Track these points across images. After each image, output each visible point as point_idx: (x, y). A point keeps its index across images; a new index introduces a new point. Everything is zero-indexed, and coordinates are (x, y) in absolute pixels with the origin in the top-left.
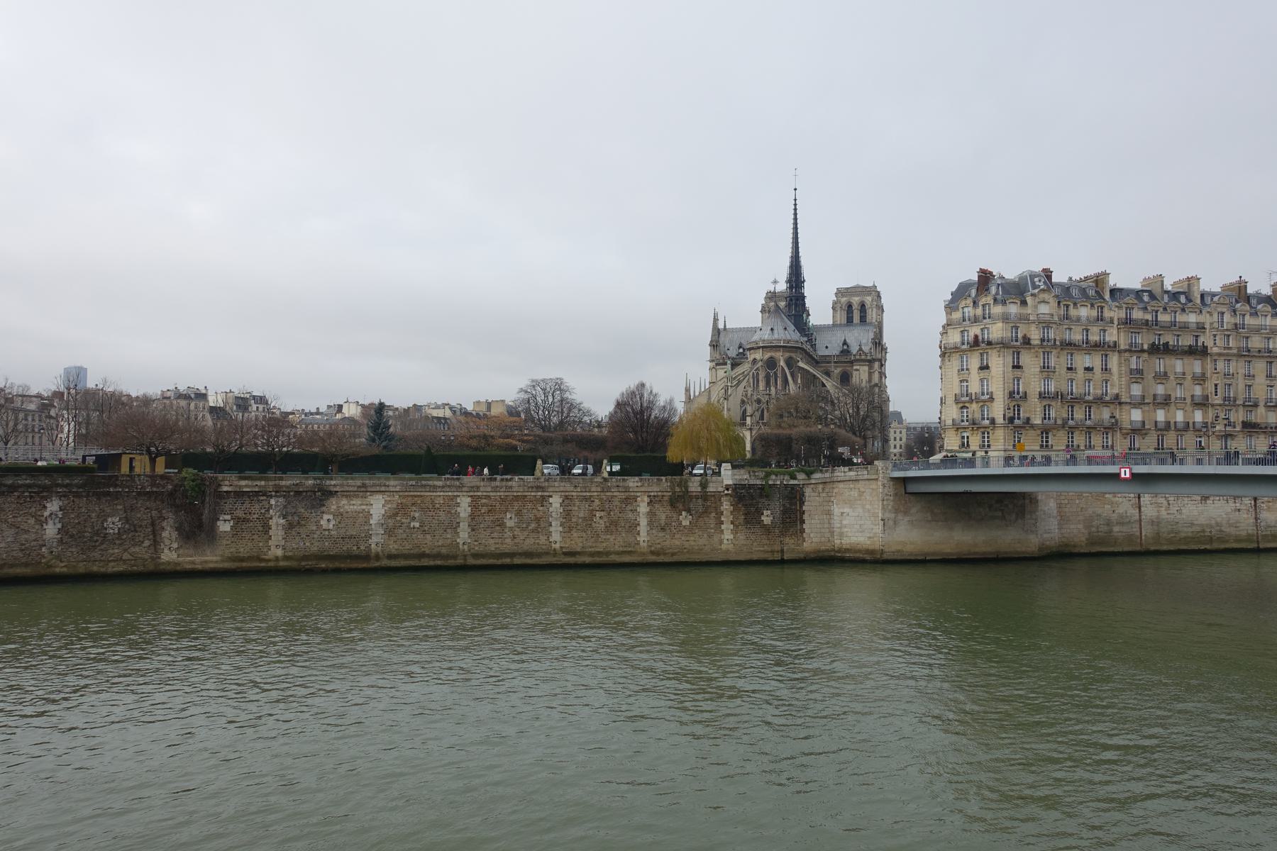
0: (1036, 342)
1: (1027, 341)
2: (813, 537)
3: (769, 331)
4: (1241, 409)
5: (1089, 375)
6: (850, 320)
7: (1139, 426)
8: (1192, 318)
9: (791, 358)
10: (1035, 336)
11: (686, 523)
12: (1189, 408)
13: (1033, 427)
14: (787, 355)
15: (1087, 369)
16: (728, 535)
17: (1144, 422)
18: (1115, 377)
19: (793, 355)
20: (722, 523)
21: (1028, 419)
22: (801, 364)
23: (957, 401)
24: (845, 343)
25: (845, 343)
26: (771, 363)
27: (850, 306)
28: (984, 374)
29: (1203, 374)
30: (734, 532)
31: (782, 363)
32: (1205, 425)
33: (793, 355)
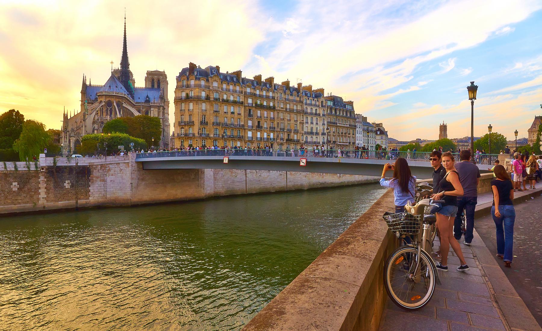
2: (96, 194)
3: (108, 87)
4: (286, 133)
5: (233, 115)
6: (153, 86)
7: (250, 139)
9: (119, 101)
11: (15, 189)
12: (268, 132)
13: (210, 138)
14: (117, 100)
17: (252, 137)
18: (243, 117)
19: (120, 100)
20: (40, 188)
21: (208, 134)
22: (124, 105)
24: (147, 97)
25: (147, 97)
26: (109, 104)
27: (153, 80)
29: (274, 118)
30: (47, 193)
31: (115, 104)
33: (120, 100)
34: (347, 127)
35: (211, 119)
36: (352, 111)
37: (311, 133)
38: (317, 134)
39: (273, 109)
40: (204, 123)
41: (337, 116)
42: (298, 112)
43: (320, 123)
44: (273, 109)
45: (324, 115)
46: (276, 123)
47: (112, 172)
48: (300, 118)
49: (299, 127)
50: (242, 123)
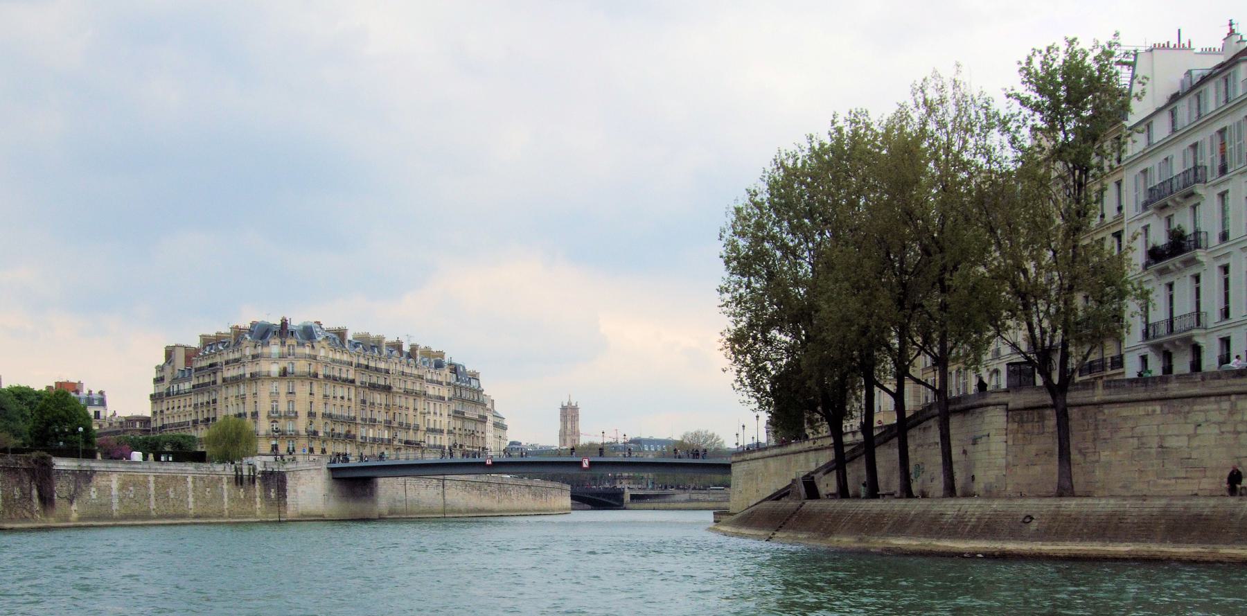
0: (321, 377)
1: (316, 376)
8: (382, 365)
10: (321, 373)
15: (342, 398)
16: (258, 506)
23: (269, 417)
28: (290, 397)
32: (389, 440)
34: (475, 420)
35: (319, 409)
36: (479, 391)
37: (434, 431)
38: (441, 431)
39: (387, 389)
40: (311, 415)
41: (463, 400)
42: (416, 395)
43: (445, 413)
44: (387, 389)
45: (450, 399)
46: (391, 413)
47: (302, 481)
48: (421, 405)
49: (419, 421)
50: (352, 415)
